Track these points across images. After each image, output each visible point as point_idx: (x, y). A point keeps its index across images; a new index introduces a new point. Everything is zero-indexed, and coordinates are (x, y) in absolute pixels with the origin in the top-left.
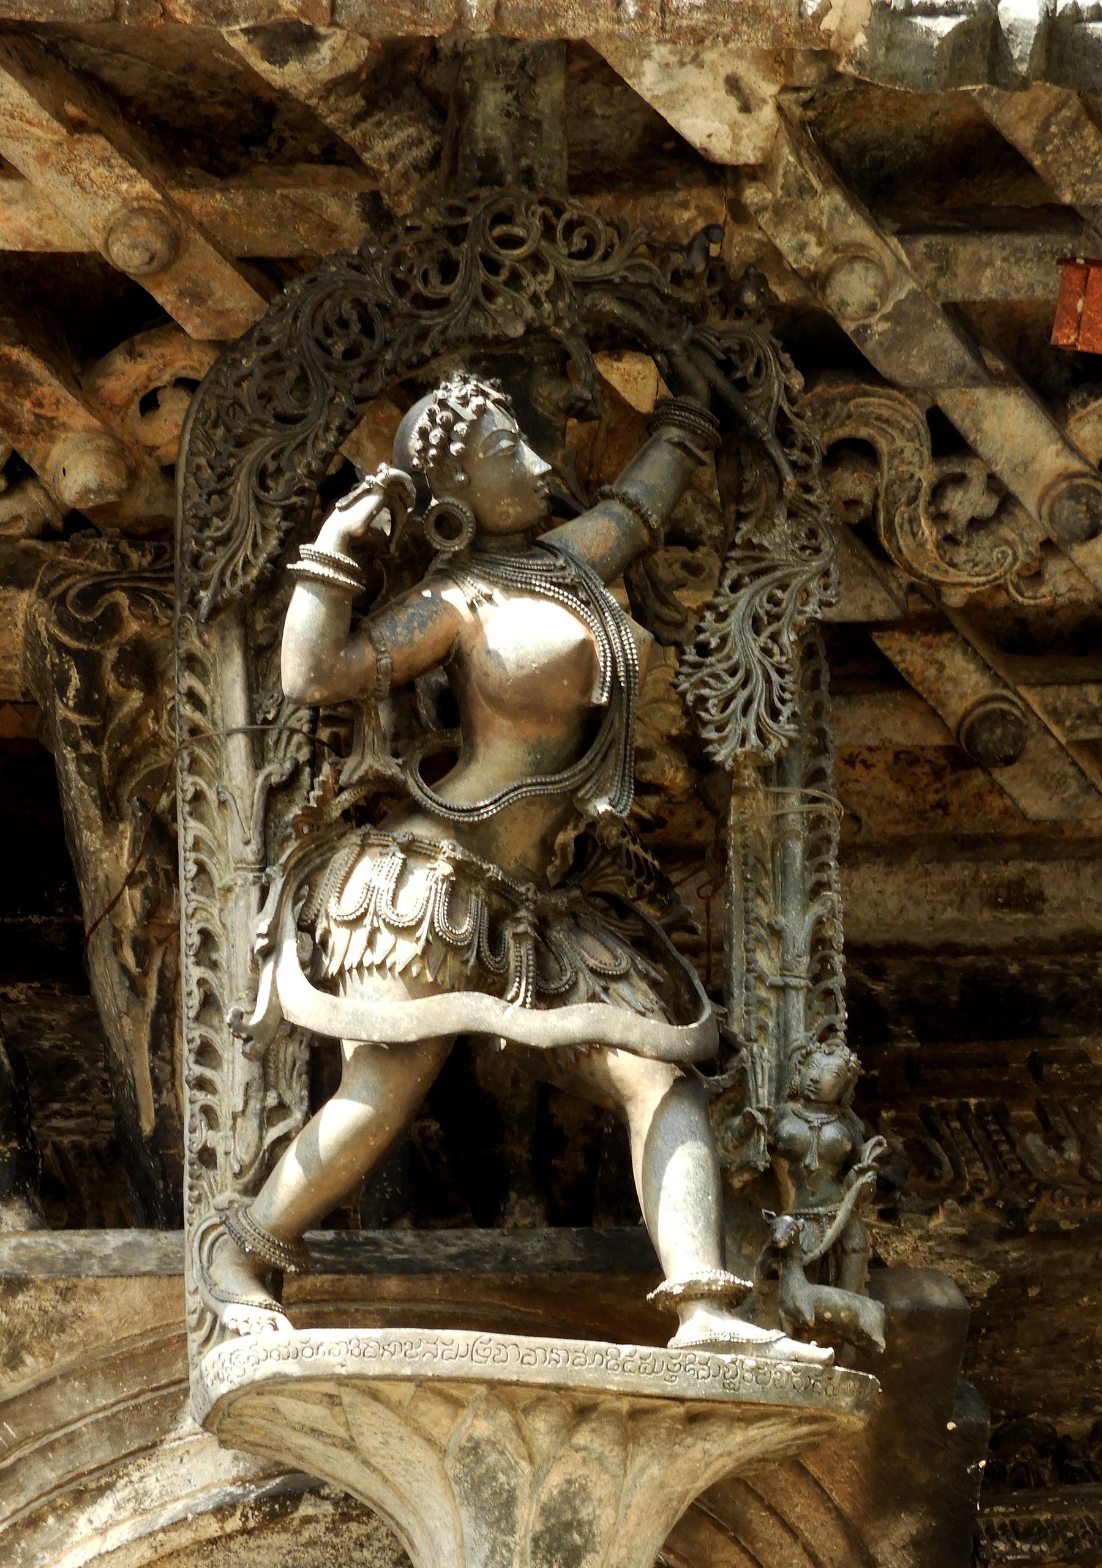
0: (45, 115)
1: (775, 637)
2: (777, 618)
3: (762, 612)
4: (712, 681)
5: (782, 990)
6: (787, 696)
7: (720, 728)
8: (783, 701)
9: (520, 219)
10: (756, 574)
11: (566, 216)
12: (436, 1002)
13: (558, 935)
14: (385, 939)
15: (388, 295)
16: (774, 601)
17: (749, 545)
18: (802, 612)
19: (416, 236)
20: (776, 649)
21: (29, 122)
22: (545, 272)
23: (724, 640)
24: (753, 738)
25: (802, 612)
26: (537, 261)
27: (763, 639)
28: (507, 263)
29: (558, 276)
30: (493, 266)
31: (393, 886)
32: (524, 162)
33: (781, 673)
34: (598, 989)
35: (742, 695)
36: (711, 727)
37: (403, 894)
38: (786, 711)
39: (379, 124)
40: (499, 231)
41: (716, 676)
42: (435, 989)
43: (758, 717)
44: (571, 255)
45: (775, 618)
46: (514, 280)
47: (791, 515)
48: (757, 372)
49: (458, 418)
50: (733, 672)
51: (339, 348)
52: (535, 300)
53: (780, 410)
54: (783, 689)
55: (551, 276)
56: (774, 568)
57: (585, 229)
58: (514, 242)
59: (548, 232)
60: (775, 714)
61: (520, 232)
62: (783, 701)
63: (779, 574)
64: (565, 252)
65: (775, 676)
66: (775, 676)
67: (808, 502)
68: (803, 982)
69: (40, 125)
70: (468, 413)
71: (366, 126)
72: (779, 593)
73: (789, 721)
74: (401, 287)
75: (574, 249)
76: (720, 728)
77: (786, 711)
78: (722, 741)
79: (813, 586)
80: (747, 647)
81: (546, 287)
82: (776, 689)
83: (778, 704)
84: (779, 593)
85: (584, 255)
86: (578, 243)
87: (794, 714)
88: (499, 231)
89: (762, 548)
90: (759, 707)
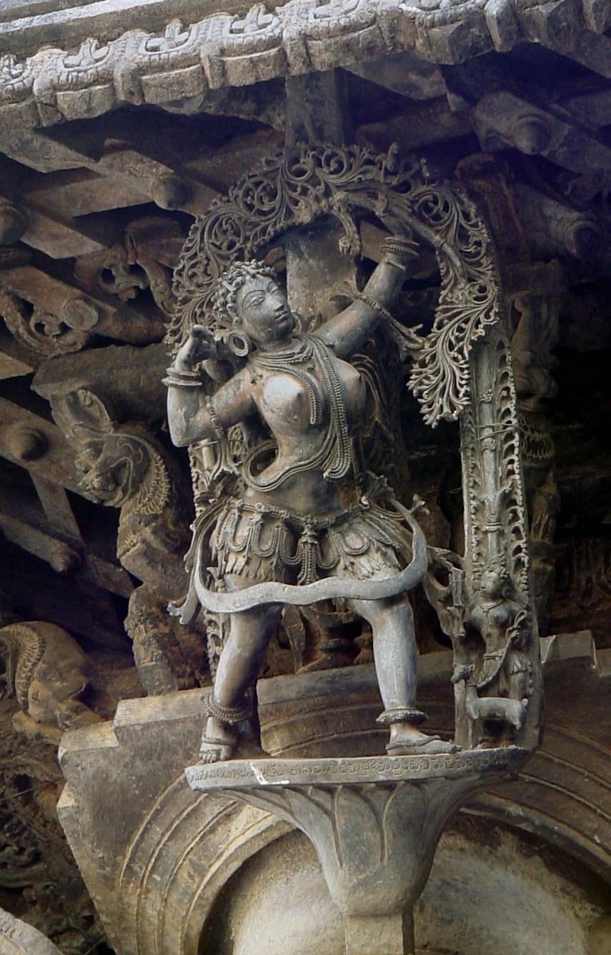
0: (81, 156)
1: (461, 351)
2: (462, 339)
3: (453, 339)
4: (426, 382)
5: (486, 532)
6: (464, 382)
7: (430, 406)
8: (462, 386)
9: (302, 160)
10: (450, 318)
11: (325, 153)
12: (251, 589)
13: (333, 536)
14: (232, 558)
15: (244, 213)
16: (461, 330)
17: (445, 302)
18: (476, 333)
19: (252, 180)
20: (460, 357)
21: (73, 160)
22: (320, 184)
23: (434, 357)
24: (446, 410)
25: (476, 333)
26: (314, 181)
27: (454, 354)
28: (299, 184)
29: (327, 185)
30: (294, 188)
31: (233, 531)
32: (317, 124)
33: (462, 370)
34: (347, 563)
35: (441, 385)
36: (425, 406)
37: (239, 534)
38: (462, 391)
39: (274, 109)
40: (294, 167)
41: (427, 378)
42: (257, 580)
43: (448, 395)
44: (332, 173)
45: (459, 340)
46: (305, 192)
47: (471, 280)
48: (446, 208)
49: (228, 292)
50: (436, 374)
51: (225, 244)
52: (317, 199)
53: (461, 226)
54: (462, 379)
55: (323, 186)
56: (460, 313)
57: (336, 158)
58: (301, 173)
59: (319, 164)
60: (457, 393)
61: (305, 167)
62: (462, 386)
63: (463, 315)
64: (328, 172)
65: (458, 373)
66: (458, 373)
67: (479, 272)
68: (495, 528)
69: (79, 160)
70: (232, 288)
71: (269, 111)
72: (463, 325)
73: (464, 395)
74: (250, 207)
75: (332, 169)
76: (430, 406)
77: (462, 391)
78: (430, 413)
79: (482, 317)
80: (446, 361)
81: (322, 192)
82: (458, 379)
83: (458, 386)
84: (463, 325)
85: (335, 172)
86: (333, 166)
87: (466, 391)
88: (294, 167)
89: (452, 303)
90: (450, 390)
